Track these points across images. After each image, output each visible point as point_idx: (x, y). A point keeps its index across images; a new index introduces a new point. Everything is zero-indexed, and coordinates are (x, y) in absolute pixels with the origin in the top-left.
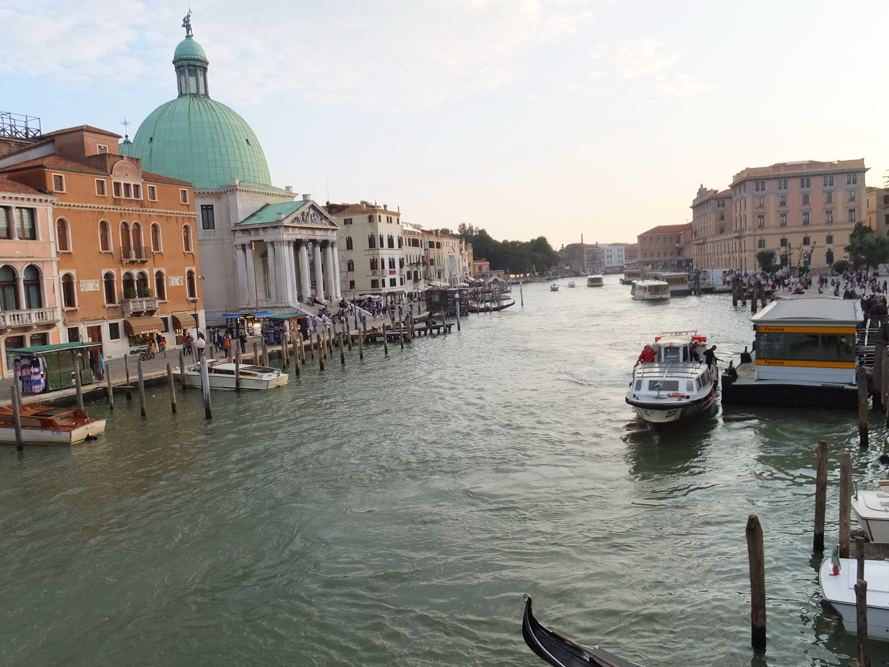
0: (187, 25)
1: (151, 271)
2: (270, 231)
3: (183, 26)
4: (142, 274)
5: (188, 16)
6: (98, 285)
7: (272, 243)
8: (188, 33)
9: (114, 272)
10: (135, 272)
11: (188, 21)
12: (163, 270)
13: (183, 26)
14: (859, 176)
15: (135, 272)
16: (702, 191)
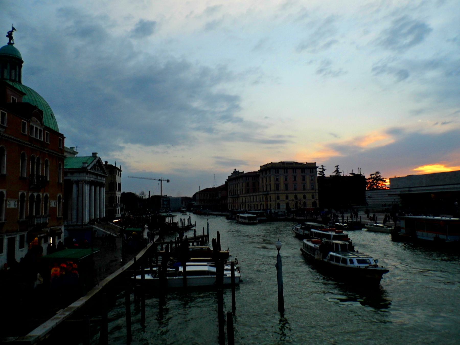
0: (10, 35)
1: (43, 195)
2: (76, 175)
3: (7, 36)
4: (38, 196)
5: (12, 31)
6: (16, 203)
7: (77, 182)
8: (10, 40)
9: (25, 193)
10: (35, 194)
11: (11, 34)
12: (48, 195)
13: (7, 36)
14: (314, 170)
15: (35, 194)
16: (235, 172)
